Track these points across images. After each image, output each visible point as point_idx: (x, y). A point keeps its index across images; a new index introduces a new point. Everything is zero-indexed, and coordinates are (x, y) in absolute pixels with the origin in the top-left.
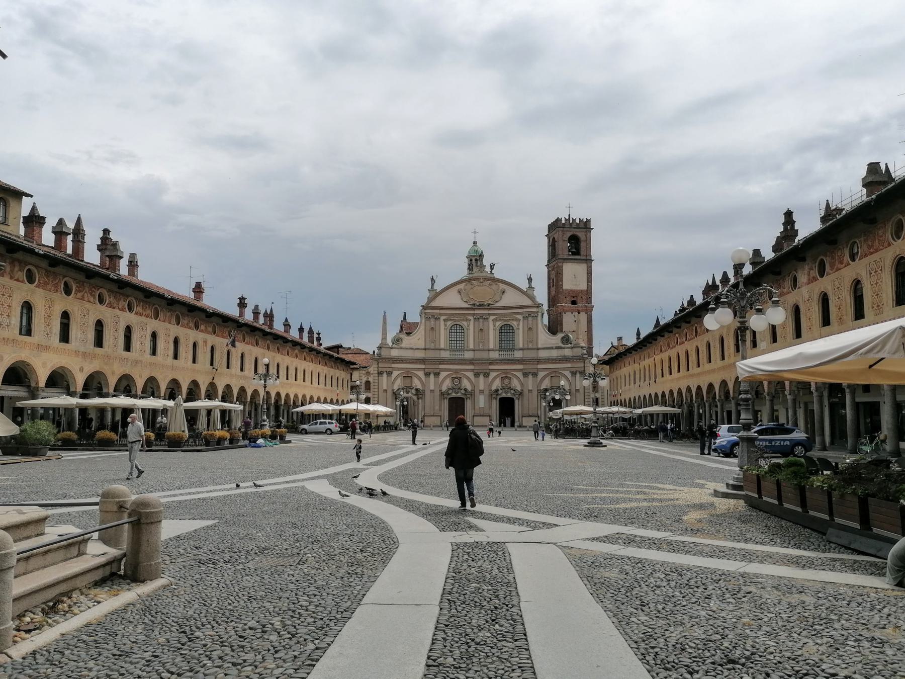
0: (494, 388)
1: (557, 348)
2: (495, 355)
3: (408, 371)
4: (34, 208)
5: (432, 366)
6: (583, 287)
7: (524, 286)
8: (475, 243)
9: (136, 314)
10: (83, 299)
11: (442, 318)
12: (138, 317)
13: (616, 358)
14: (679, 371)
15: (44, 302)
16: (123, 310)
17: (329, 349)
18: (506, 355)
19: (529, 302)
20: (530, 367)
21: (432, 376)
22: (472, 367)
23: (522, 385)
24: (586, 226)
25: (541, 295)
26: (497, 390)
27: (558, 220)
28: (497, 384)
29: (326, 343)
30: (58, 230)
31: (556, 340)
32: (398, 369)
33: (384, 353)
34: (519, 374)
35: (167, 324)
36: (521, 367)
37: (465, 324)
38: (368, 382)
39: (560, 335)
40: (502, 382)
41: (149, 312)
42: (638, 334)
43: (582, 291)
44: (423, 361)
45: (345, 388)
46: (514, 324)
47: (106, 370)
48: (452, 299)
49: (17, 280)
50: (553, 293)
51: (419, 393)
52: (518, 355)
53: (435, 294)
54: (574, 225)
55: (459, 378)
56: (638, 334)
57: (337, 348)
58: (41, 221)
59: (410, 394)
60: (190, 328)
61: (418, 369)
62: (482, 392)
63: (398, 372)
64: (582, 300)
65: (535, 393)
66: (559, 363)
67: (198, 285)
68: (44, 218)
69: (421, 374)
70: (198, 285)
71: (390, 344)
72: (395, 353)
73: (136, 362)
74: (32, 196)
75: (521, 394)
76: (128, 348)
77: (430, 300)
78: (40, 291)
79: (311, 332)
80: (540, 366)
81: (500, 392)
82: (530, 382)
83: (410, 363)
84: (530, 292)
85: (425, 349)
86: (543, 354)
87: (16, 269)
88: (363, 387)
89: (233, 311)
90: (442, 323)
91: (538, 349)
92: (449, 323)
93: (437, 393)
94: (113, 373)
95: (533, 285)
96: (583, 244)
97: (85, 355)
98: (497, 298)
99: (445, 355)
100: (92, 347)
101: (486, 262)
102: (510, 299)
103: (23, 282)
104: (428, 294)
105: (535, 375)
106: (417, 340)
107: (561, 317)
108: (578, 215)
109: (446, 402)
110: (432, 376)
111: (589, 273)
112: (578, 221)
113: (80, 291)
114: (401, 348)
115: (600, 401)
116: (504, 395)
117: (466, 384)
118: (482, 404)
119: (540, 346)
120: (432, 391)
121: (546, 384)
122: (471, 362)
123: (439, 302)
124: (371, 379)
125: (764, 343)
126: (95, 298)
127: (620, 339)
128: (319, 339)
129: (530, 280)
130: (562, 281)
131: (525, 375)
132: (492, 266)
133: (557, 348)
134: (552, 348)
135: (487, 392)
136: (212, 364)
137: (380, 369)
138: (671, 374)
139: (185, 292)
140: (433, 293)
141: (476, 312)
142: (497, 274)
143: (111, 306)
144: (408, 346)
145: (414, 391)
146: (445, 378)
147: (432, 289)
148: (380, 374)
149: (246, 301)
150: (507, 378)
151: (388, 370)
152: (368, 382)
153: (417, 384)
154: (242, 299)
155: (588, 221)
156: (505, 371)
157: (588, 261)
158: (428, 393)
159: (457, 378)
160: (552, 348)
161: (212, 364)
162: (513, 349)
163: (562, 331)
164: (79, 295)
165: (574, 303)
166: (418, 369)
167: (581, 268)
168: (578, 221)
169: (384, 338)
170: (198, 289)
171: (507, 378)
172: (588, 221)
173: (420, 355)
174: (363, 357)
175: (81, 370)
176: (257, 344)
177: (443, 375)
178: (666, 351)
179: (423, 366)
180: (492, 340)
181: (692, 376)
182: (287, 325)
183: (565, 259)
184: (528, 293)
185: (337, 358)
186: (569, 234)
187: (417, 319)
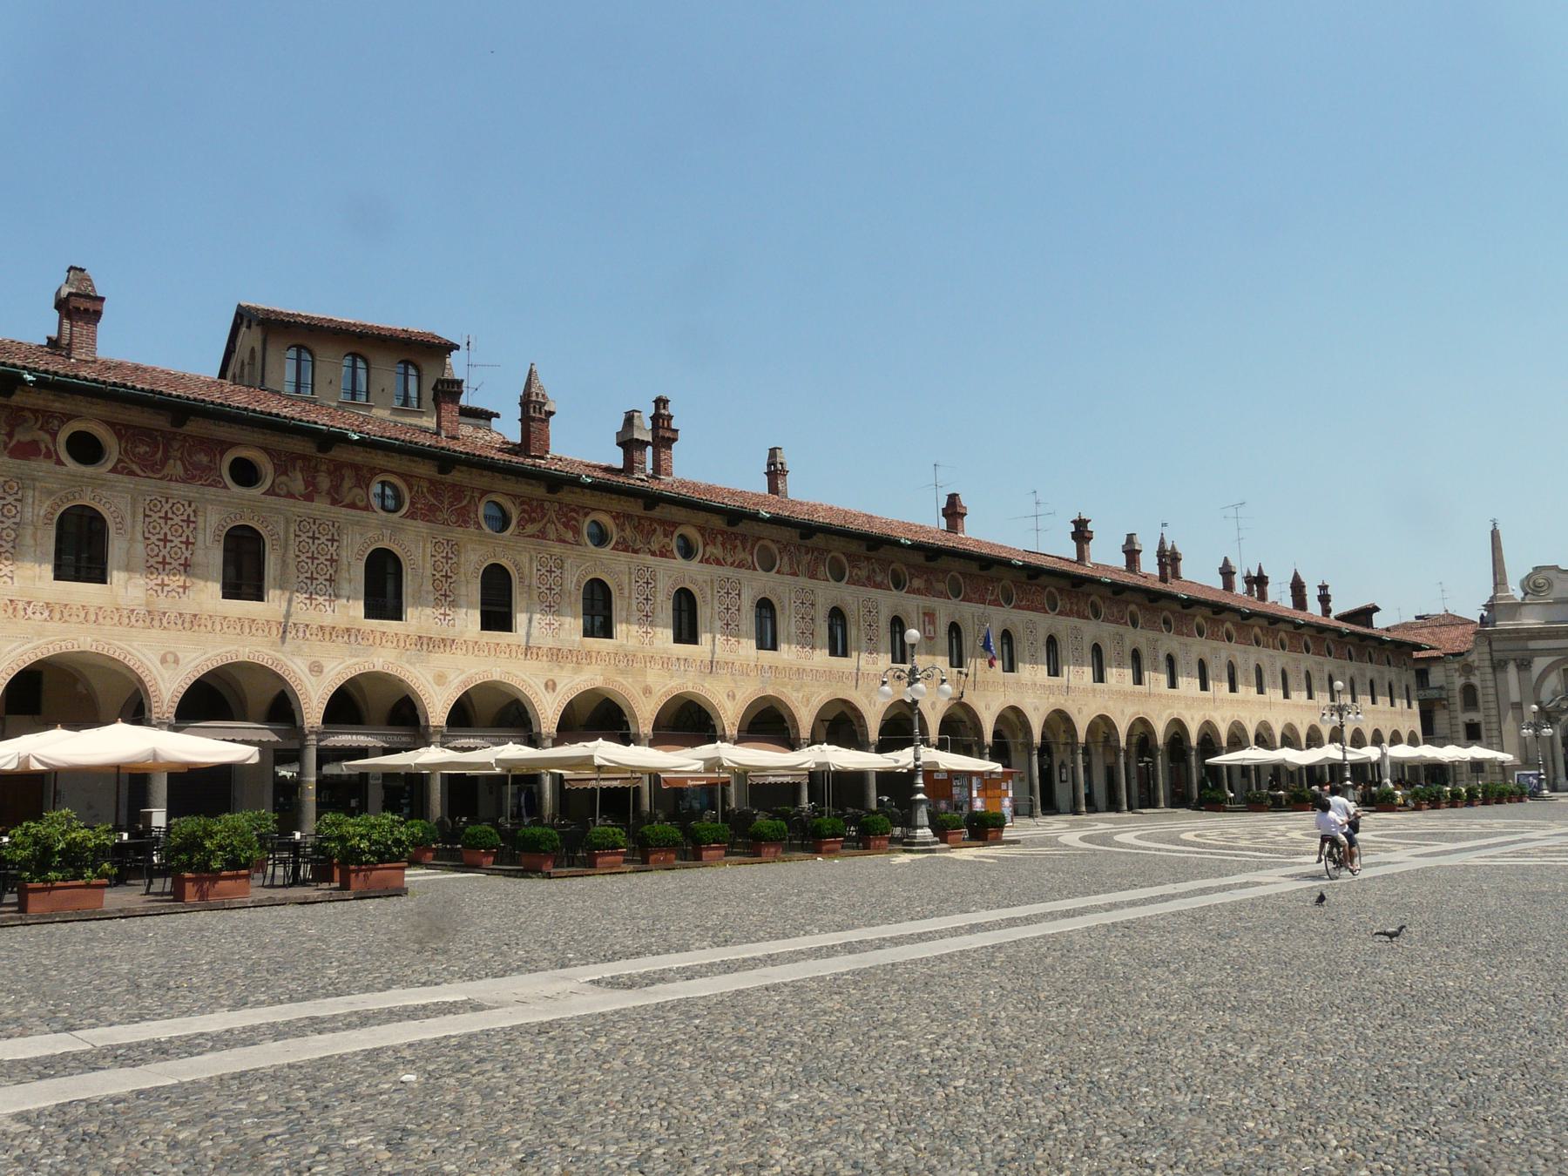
10: (542, 535)
15: (429, 548)
17: (1343, 618)
35: (803, 581)
41: (741, 555)
49: (353, 506)
57: (1364, 615)
60: (878, 586)
63: (1549, 660)
67: (953, 499)
70: (953, 499)
71: (1518, 595)
79: (1298, 588)
87: (347, 484)
88: (1458, 700)
97: (556, 655)
128: (1324, 599)
139: (916, 515)
143: (624, 546)
164: (531, 529)
170: (953, 511)
174: (1455, 632)
175: (551, 686)
176: (1097, 615)
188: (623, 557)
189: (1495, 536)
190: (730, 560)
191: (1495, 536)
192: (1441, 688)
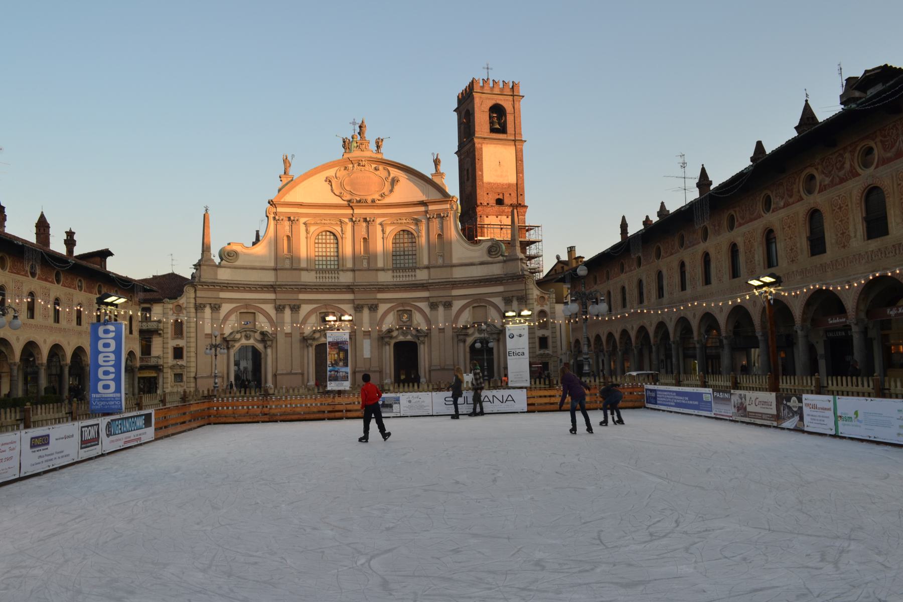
0: (385, 328)
1: (482, 263)
3: (247, 304)
6: (512, 179)
7: (428, 170)
11: (302, 220)
18: (404, 278)
21: (288, 312)
22: (350, 296)
23: (428, 322)
25: (453, 187)
26: (390, 331)
28: (389, 322)
32: (231, 300)
33: (206, 276)
34: (423, 306)
36: (425, 294)
40: (400, 318)
42: (624, 226)
43: (509, 185)
44: (272, 288)
51: (265, 337)
52: (422, 276)
54: (496, 91)
56: (624, 226)
59: (251, 342)
61: (265, 301)
62: (367, 334)
65: (449, 333)
69: (270, 309)
71: (217, 260)
72: (224, 275)
80: (455, 292)
81: (395, 334)
82: (441, 318)
83: (251, 291)
84: (436, 180)
85: (275, 269)
86: (459, 274)
88: (170, 331)
90: (303, 228)
93: (297, 337)
96: (510, 119)
101: (370, 136)
105: (448, 305)
108: (501, 74)
110: (288, 312)
111: (519, 160)
114: (235, 268)
115: (550, 341)
116: (401, 338)
118: (367, 354)
119: (455, 261)
121: (465, 319)
122: (350, 288)
123: (297, 195)
124: (183, 318)
127: (571, 250)
129: (437, 162)
130: (482, 170)
131: (433, 306)
133: (482, 263)
134: (472, 264)
135: (375, 335)
137: (199, 301)
144: (246, 264)
148: (199, 308)
150: (405, 311)
151: (213, 301)
153: (263, 324)
156: (403, 302)
157: (517, 141)
158: (281, 339)
160: (472, 264)
162: (414, 269)
166: (265, 301)
169: (206, 249)
171: (405, 311)
173: (269, 278)
177: (305, 309)
179: (272, 296)
186: (490, 103)
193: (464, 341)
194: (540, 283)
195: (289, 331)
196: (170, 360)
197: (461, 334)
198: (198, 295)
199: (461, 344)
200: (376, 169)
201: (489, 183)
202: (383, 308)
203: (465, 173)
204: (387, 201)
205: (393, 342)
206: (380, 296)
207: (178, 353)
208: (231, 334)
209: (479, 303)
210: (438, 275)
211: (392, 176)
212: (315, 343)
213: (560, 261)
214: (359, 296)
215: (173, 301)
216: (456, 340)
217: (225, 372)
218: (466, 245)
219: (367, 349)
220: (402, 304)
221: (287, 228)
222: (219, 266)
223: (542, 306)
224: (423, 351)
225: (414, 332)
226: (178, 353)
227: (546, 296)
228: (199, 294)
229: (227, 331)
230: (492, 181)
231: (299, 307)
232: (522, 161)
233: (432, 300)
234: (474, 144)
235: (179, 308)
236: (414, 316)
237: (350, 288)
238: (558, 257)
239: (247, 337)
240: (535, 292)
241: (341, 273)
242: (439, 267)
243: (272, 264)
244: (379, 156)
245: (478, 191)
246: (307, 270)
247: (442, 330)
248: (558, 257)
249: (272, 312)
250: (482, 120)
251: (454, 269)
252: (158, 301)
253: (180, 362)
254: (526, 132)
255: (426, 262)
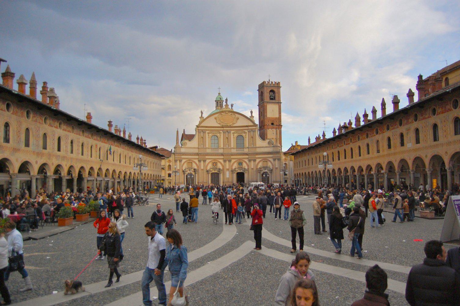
0: (234, 168)
1: (266, 147)
2: (234, 151)
3: (190, 159)
4: (8, 68)
5: (201, 156)
6: (277, 116)
7: (248, 115)
8: (219, 94)
9: (63, 130)
10: (36, 121)
11: (207, 132)
12: (64, 132)
13: (297, 152)
14: (345, 158)
16: (57, 128)
18: (240, 151)
19: (251, 124)
20: (252, 156)
21: (202, 162)
22: (222, 157)
24: (278, 85)
27: (264, 82)
29: (149, 145)
30: (20, 81)
31: (265, 143)
32: (185, 158)
33: (178, 151)
34: (246, 160)
36: (247, 157)
37: (218, 135)
38: (170, 166)
39: (267, 141)
42: (309, 140)
44: (197, 154)
45: (159, 170)
46: (244, 135)
47: (49, 162)
48: (212, 122)
50: (262, 119)
52: (246, 151)
53: (203, 120)
54: (272, 85)
55: (216, 164)
56: (309, 140)
58: (12, 75)
62: (228, 170)
64: (277, 124)
65: (255, 169)
66: (267, 155)
68: (14, 74)
69: (197, 161)
73: (64, 158)
74: (6, 61)
75: (248, 170)
76: (59, 150)
77: (200, 123)
78: (14, 117)
79: (142, 139)
80: (257, 156)
81: (237, 170)
84: (251, 119)
86: (258, 150)
88: (167, 168)
89: (107, 128)
91: (256, 148)
92: (210, 135)
93: (205, 171)
94: (53, 164)
95: (253, 115)
96: (277, 95)
98: (234, 122)
99: (208, 151)
100: (42, 149)
101: (229, 103)
102: (242, 122)
103: (4, 111)
104: (199, 120)
105: (255, 161)
106: (194, 143)
107: (267, 131)
108: (274, 80)
109: (210, 175)
110: (202, 162)
112: (274, 83)
113: (34, 117)
114: (186, 148)
117: (220, 166)
119: (257, 146)
120: (202, 170)
121: (260, 165)
122: (222, 155)
124: (171, 164)
125: (410, 144)
126: (42, 121)
127: (296, 142)
128: (145, 143)
129: (252, 112)
130: (266, 113)
131: (250, 161)
132: (232, 106)
133: (266, 147)
134: (263, 147)
135: (230, 170)
136: (100, 158)
137: (176, 159)
138: (339, 159)
139: (82, 117)
140: (202, 119)
141: (224, 129)
142: (235, 109)
145: (193, 170)
146: (209, 163)
147: (202, 117)
148: (176, 161)
149: (112, 123)
152: (170, 166)
153: (195, 166)
154: (110, 122)
155: (279, 83)
156: (240, 159)
157: (279, 103)
158: (200, 171)
159: (240, 164)
161: (100, 158)
162: (243, 148)
163: (267, 138)
164: (35, 119)
165: (272, 124)
167: (276, 107)
168: (274, 83)
172: (279, 83)
173: (196, 151)
175: (37, 162)
178: (336, 148)
179: (197, 157)
180: (233, 143)
181: (356, 161)
182: (130, 136)
183: (267, 102)
184: (250, 119)
185: (157, 153)
187: (194, 133)
188: (50, 128)
189: (178, 131)
190: (67, 130)
191: (178, 131)
192: (164, 165)
193: (260, 173)
194: (285, 154)
195: (203, 168)
196: (167, 178)
197: (259, 170)
198: (175, 157)
199: (259, 174)
200: (231, 115)
201: (269, 118)
202: (233, 161)
203: (261, 113)
204: (235, 125)
205: (236, 172)
206: (232, 157)
207: (170, 175)
208: (185, 169)
209: (265, 160)
210: (252, 151)
211: (236, 117)
212: (211, 172)
213: (292, 146)
214: (225, 157)
215: (168, 159)
216: (257, 172)
217: (183, 181)
218: (261, 141)
219: (228, 174)
220: (239, 160)
221: (202, 134)
222: (181, 147)
223: (285, 162)
224: (246, 176)
225: (244, 170)
226: (170, 175)
227: (287, 159)
228: (176, 157)
229: (184, 169)
230: (270, 117)
231: (206, 160)
232: (281, 109)
233: (249, 159)
234: (264, 104)
235: (170, 161)
236: (243, 164)
237: (222, 155)
238: (292, 144)
239: (190, 170)
240: (283, 157)
241: (219, 149)
242: (252, 148)
243: (197, 146)
244: (232, 110)
245: (265, 120)
246: (208, 148)
247: (252, 169)
248: (292, 144)
249: (197, 162)
250: (267, 95)
251: (257, 149)
252: (163, 159)
253: (170, 178)
254: (282, 101)
255: (247, 146)
